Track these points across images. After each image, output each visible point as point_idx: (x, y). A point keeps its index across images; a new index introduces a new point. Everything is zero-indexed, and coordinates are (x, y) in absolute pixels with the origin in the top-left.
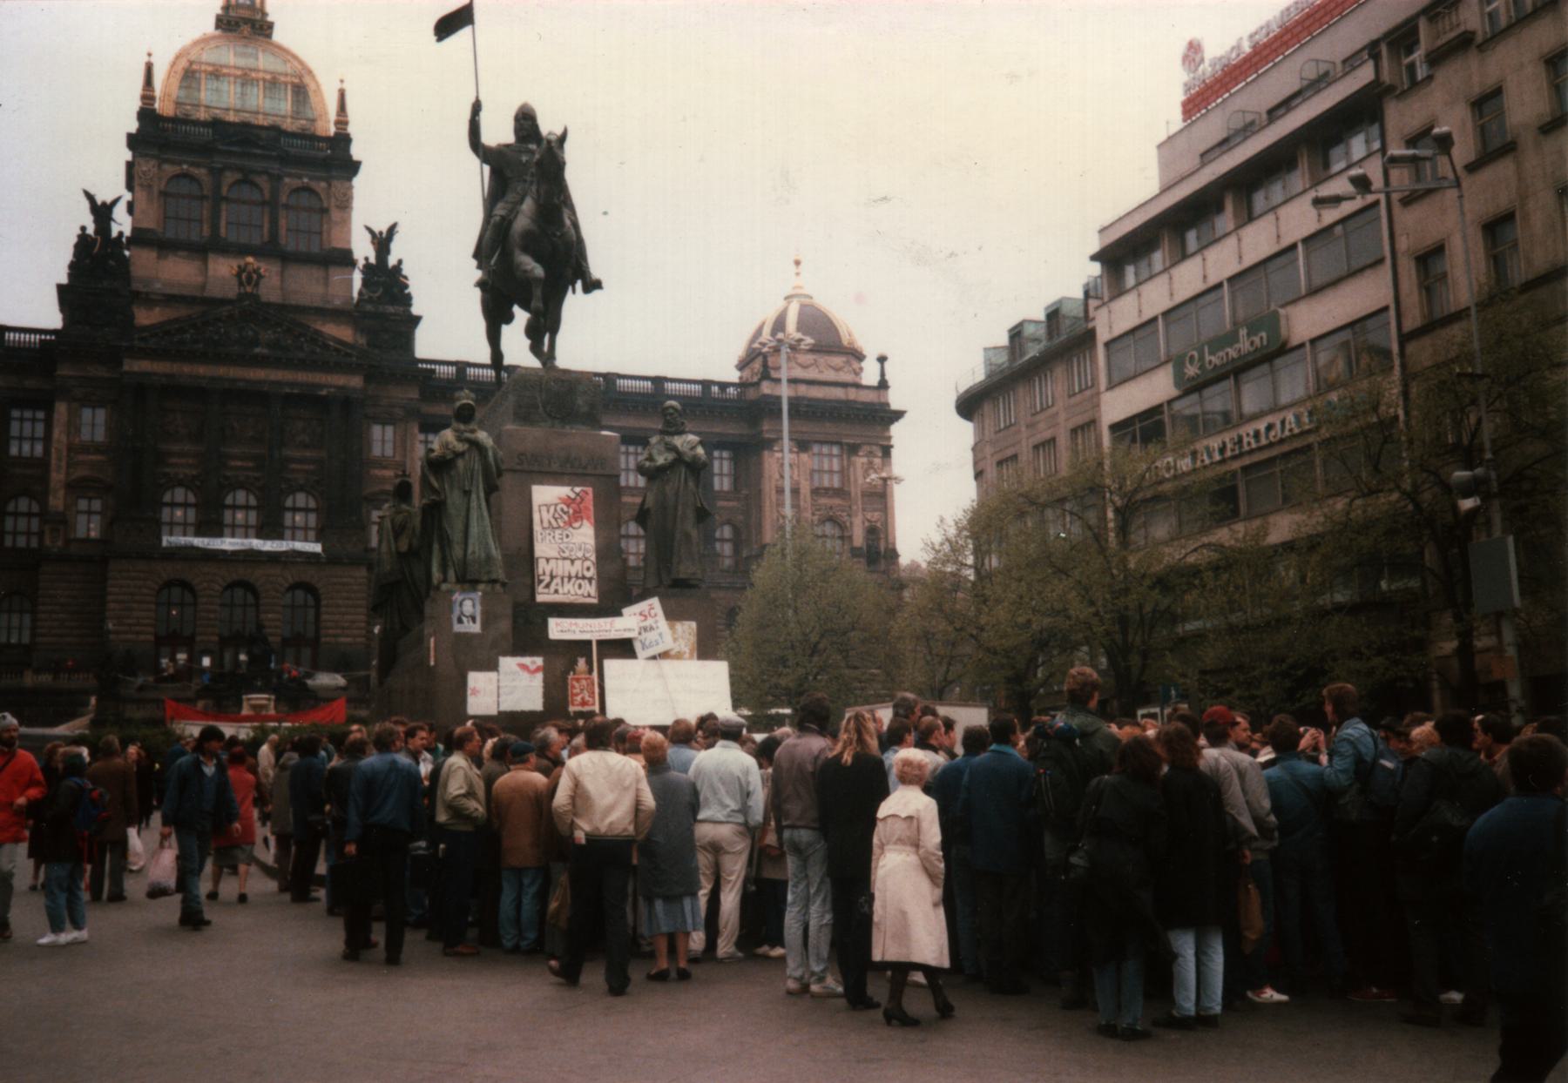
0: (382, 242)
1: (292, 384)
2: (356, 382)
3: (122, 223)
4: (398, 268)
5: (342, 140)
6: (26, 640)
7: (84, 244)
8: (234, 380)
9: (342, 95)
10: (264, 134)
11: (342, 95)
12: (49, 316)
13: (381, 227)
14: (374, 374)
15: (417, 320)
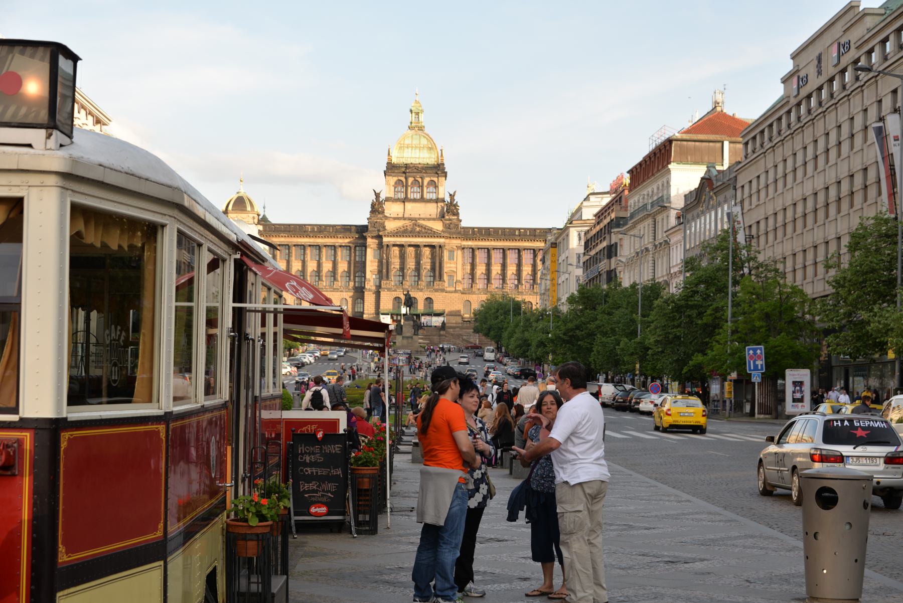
0: (452, 196)
1: (427, 242)
2: (442, 240)
3: (383, 197)
4: (456, 205)
5: (443, 164)
6: (362, 311)
7: (373, 206)
8: (410, 242)
9: (441, 150)
10: (420, 166)
11: (441, 150)
12: (365, 223)
13: (452, 193)
14: (447, 238)
15: (461, 221)
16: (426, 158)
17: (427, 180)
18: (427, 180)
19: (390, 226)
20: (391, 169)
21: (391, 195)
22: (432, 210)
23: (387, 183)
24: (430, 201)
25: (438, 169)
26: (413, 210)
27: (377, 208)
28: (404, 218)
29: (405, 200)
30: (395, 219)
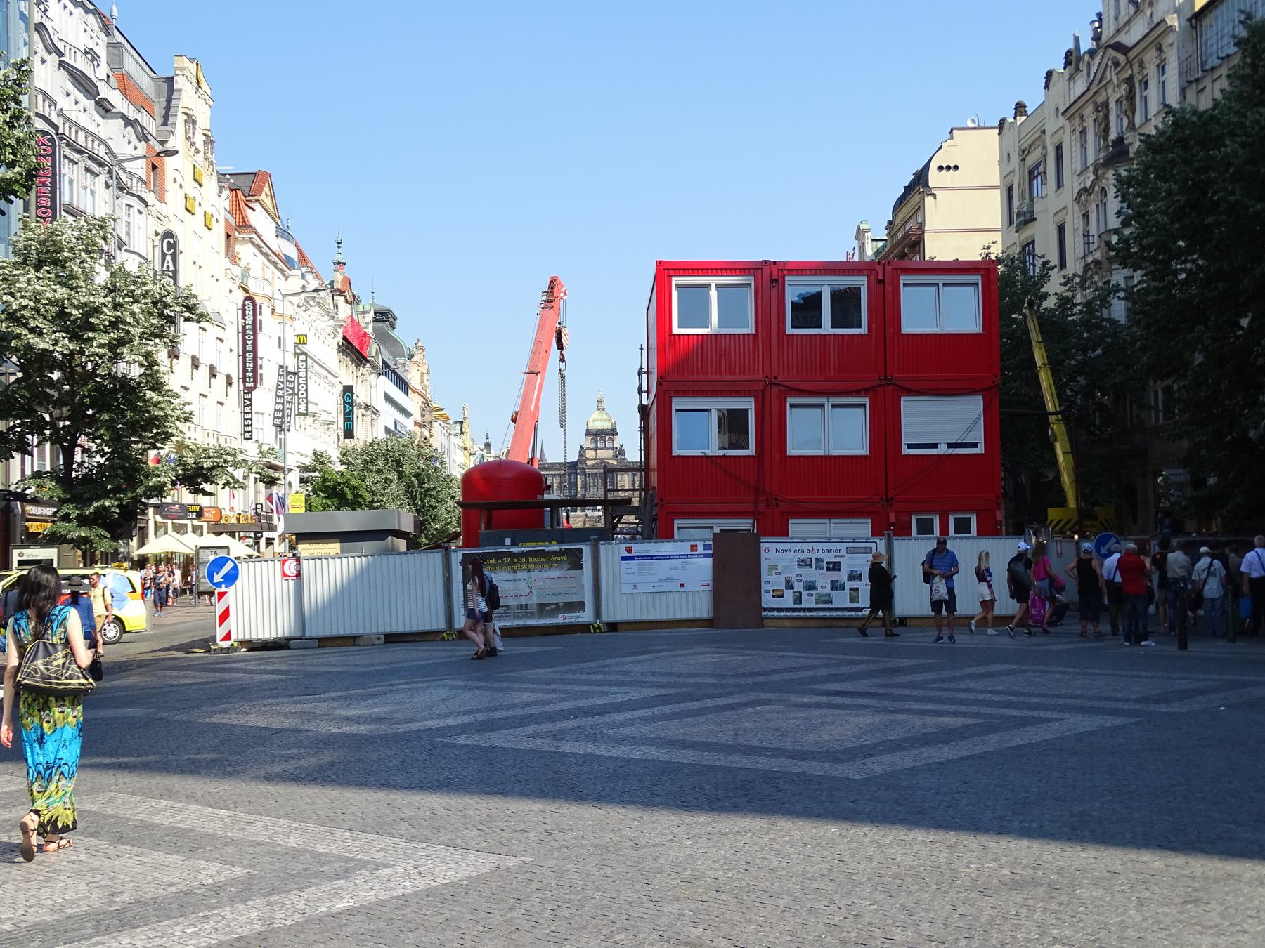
0: (621, 446)
7: (580, 452)
16: (605, 425)
17: (607, 438)
18: (607, 438)
19: (589, 463)
20: (588, 433)
21: (590, 446)
22: (611, 453)
23: (587, 440)
24: (609, 449)
25: (613, 432)
26: (602, 454)
27: (582, 452)
28: (596, 459)
29: (596, 449)
30: (592, 459)
